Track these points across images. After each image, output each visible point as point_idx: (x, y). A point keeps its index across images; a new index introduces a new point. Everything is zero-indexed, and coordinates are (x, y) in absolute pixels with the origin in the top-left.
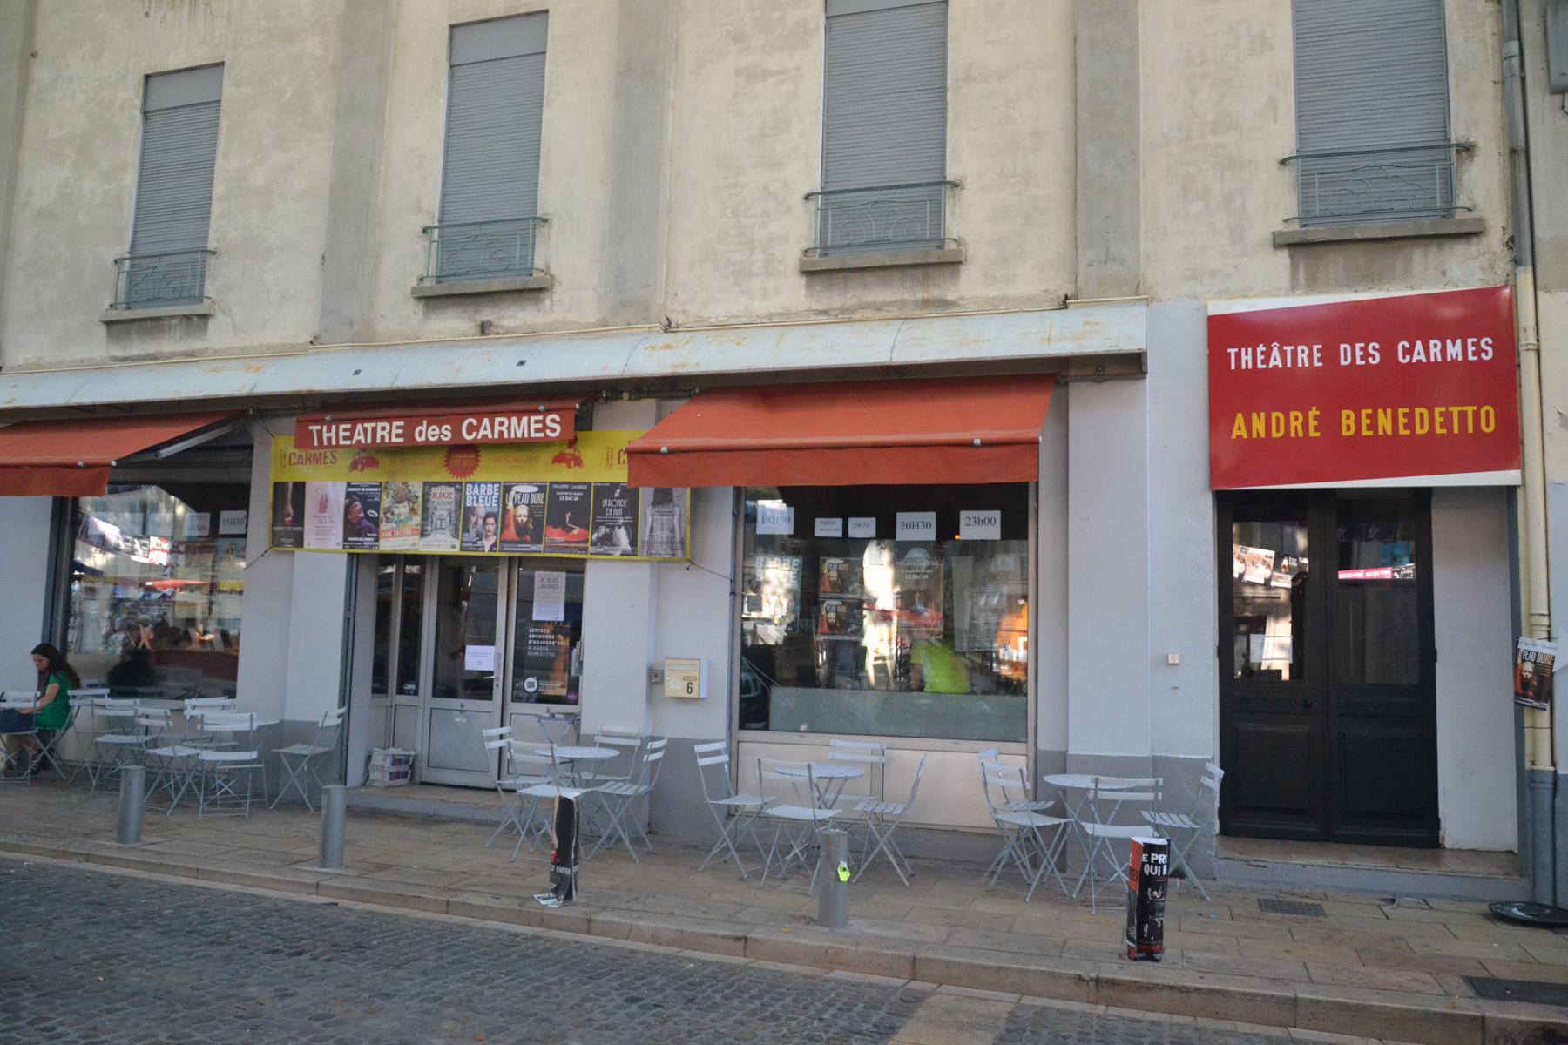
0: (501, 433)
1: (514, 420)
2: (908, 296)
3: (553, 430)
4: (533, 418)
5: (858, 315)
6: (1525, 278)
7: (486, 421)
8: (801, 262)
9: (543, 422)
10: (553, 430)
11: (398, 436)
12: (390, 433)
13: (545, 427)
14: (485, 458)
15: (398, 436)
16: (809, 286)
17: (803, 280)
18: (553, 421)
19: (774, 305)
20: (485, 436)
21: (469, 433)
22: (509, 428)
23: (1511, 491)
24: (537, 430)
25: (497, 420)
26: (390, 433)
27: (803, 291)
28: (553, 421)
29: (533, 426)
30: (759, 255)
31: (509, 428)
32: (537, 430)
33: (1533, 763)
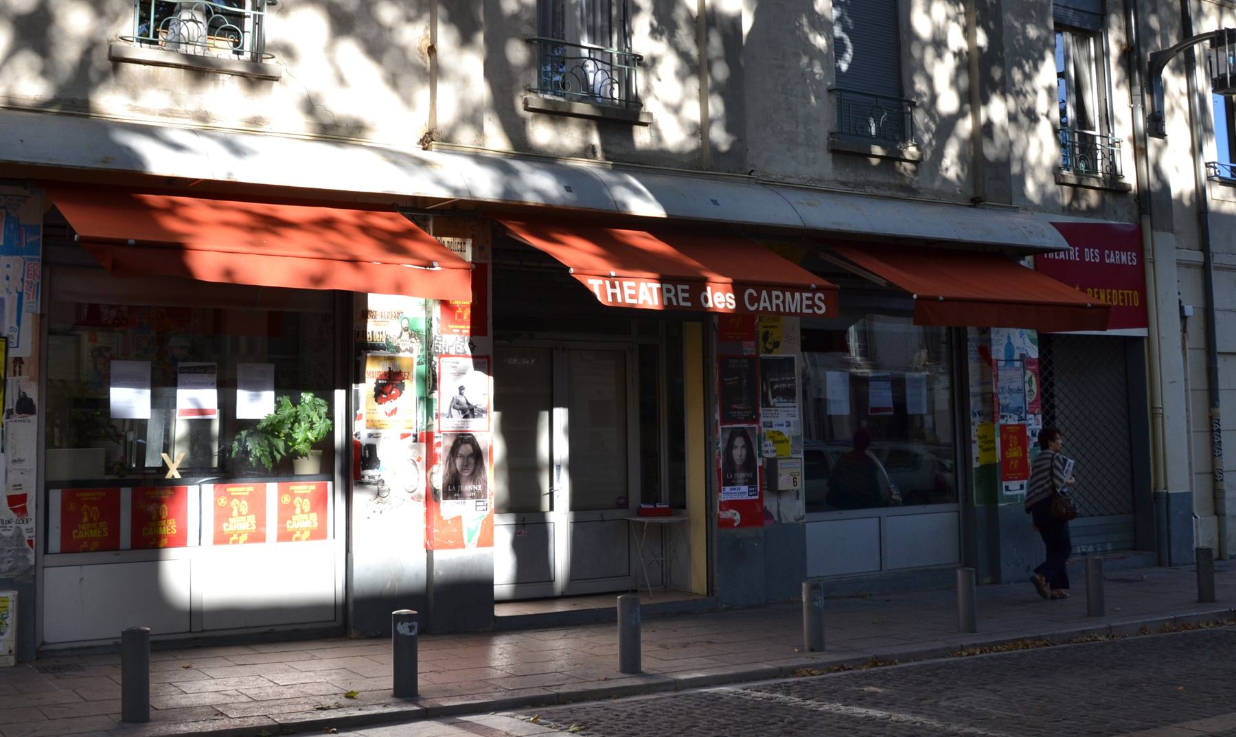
0: (777, 305)
1: (788, 295)
2: (891, 181)
3: (820, 308)
4: (805, 295)
5: (869, 190)
6: (1146, 223)
7: (764, 293)
8: (831, 143)
9: (812, 299)
10: (820, 308)
11: (685, 299)
12: (676, 295)
13: (814, 304)
14: (1213, 520)
15: (685, 299)
16: (834, 161)
17: (830, 157)
18: (820, 299)
19: (808, 172)
20: (765, 308)
21: (752, 305)
22: (784, 302)
23: (1141, 339)
24: (808, 307)
25: (774, 293)
26: (676, 295)
27: (831, 165)
28: (820, 299)
29: (805, 302)
30: (801, 129)
31: (784, 302)
32: (808, 307)
33: (1166, 488)
